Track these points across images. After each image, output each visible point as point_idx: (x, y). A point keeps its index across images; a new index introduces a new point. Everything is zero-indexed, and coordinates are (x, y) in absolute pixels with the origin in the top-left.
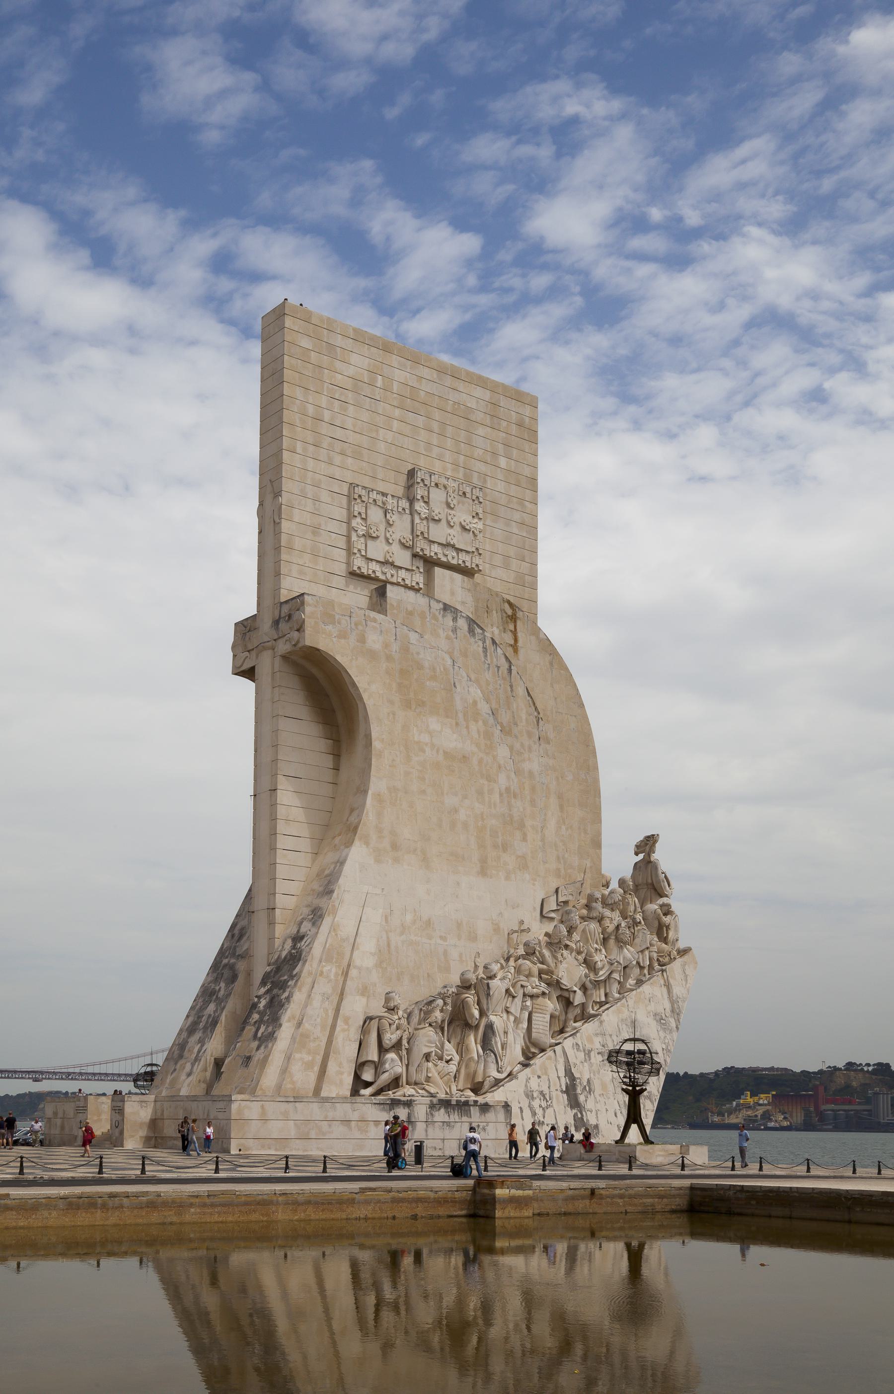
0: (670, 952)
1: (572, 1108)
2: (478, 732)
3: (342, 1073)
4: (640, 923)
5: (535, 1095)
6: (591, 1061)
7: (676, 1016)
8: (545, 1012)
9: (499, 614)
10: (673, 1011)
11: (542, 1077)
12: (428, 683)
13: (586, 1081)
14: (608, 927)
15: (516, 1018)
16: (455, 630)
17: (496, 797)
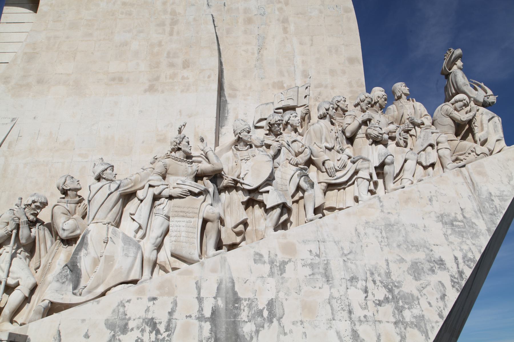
4: (423, 124)
6: (284, 275)
8: (191, 215)
10: (481, 211)
14: (349, 124)
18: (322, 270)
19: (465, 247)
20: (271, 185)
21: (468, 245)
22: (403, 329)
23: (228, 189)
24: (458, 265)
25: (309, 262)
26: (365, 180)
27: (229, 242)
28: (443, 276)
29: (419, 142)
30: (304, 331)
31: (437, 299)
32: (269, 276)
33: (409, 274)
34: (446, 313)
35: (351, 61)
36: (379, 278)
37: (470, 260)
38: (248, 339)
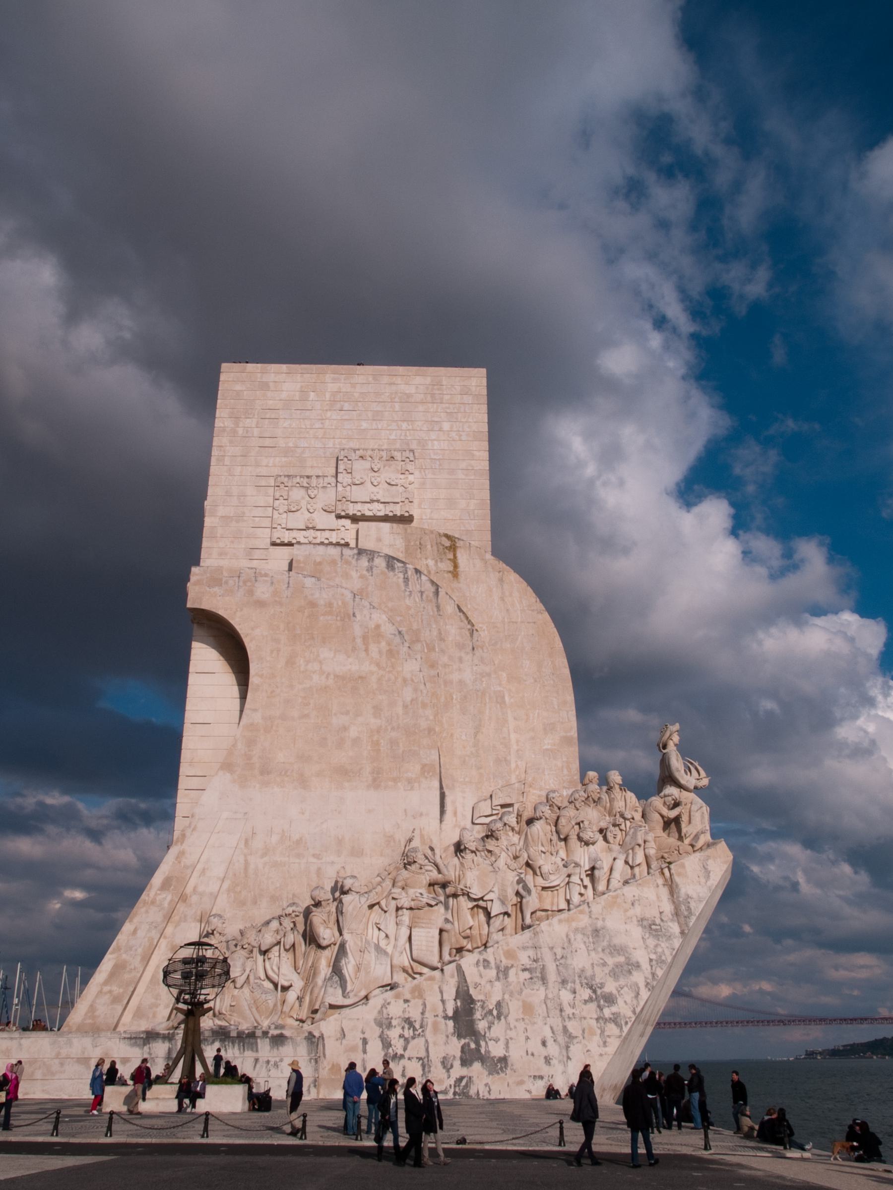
0: (678, 847)
1: (460, 1036)
2: (380, 652)
3: (157, 1006)
4: (633, 819)
5: (394, 1022)
7: (682, 919)
8: (430, 925)
9: (435, 548)
11: (413, 1002)
12: (322, 618)
13: (495, 1003)
14: (563, 826)
15: (387, 936)
16: (370, 569)
17: (400, 710)
18: (538, 975)
19: (659, 950)
20: (493, 892)
21: (662, 948)
22: (603, 1024)
23: (455, 896)
24: (652, 966)
25: (528, 967)
26: (576, 885)
27: (458, 946)
28: (638, 978)
29: (628, 838)
30: (525, 1026)
31: (632, 998)
32: (496, 980)
33: (610, 976)
34: (638, 1010)
35: (567, 740)
36: (586, 981)
37: (663, 962)
38: (483, 1034)
